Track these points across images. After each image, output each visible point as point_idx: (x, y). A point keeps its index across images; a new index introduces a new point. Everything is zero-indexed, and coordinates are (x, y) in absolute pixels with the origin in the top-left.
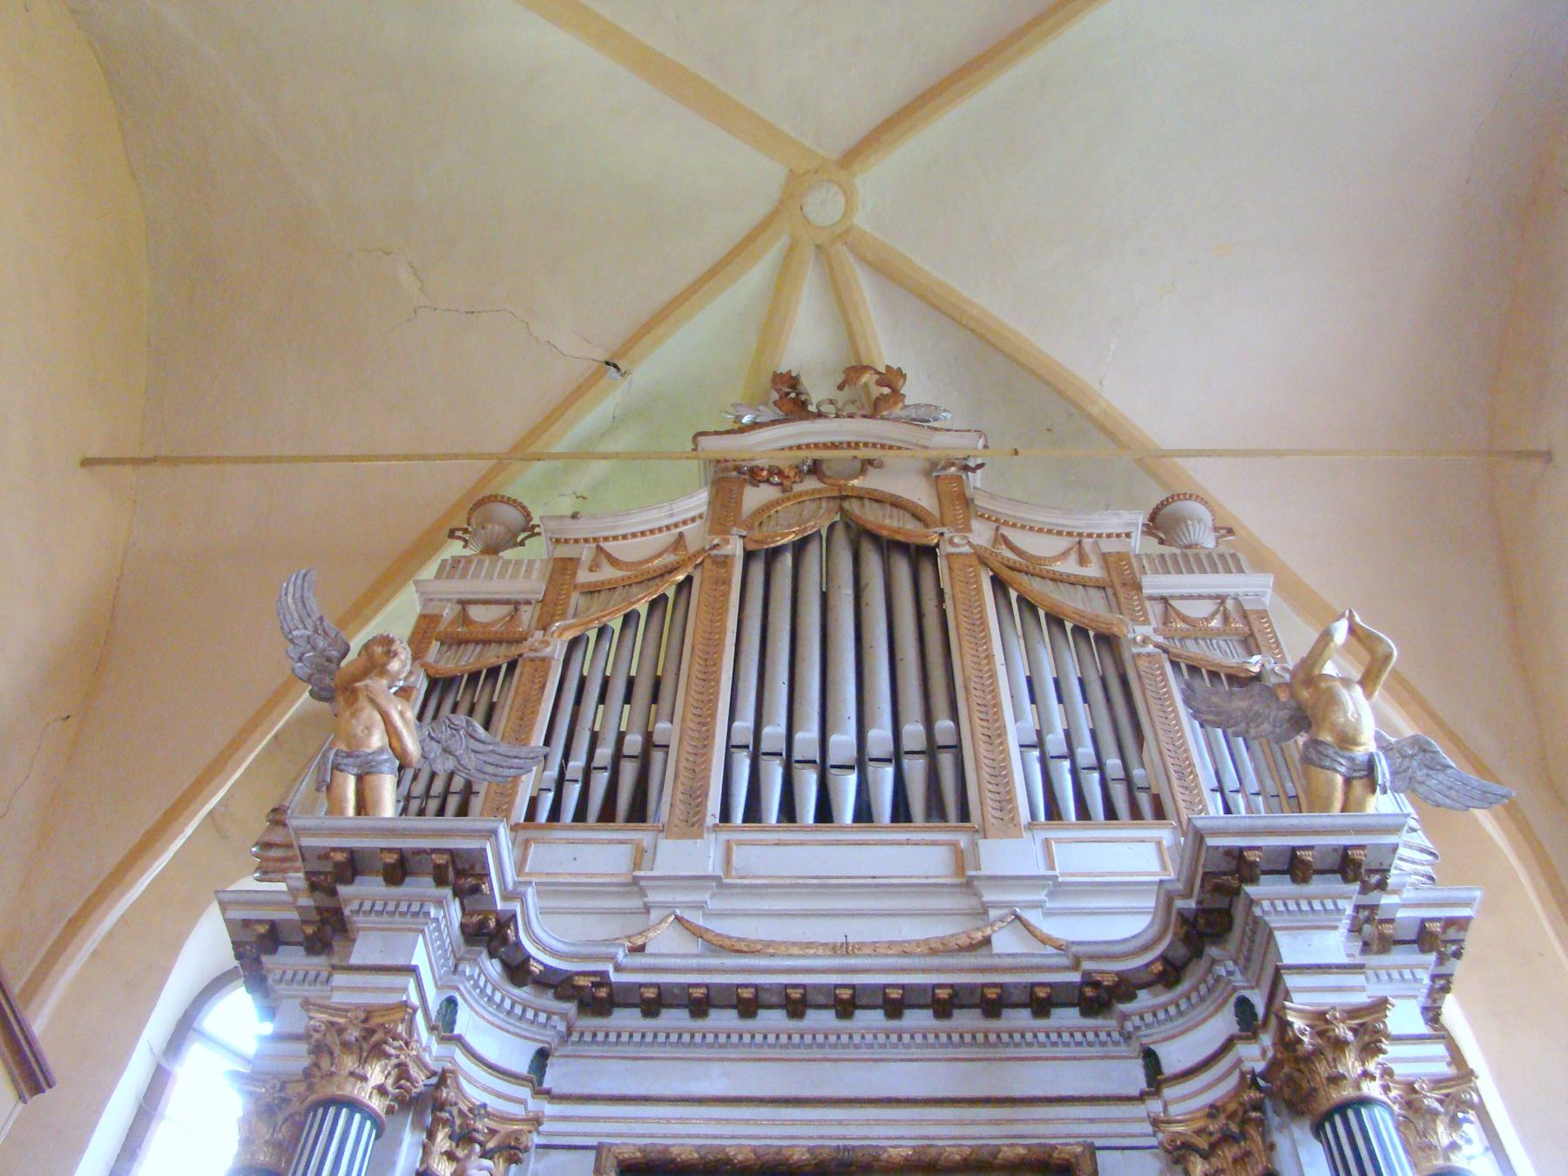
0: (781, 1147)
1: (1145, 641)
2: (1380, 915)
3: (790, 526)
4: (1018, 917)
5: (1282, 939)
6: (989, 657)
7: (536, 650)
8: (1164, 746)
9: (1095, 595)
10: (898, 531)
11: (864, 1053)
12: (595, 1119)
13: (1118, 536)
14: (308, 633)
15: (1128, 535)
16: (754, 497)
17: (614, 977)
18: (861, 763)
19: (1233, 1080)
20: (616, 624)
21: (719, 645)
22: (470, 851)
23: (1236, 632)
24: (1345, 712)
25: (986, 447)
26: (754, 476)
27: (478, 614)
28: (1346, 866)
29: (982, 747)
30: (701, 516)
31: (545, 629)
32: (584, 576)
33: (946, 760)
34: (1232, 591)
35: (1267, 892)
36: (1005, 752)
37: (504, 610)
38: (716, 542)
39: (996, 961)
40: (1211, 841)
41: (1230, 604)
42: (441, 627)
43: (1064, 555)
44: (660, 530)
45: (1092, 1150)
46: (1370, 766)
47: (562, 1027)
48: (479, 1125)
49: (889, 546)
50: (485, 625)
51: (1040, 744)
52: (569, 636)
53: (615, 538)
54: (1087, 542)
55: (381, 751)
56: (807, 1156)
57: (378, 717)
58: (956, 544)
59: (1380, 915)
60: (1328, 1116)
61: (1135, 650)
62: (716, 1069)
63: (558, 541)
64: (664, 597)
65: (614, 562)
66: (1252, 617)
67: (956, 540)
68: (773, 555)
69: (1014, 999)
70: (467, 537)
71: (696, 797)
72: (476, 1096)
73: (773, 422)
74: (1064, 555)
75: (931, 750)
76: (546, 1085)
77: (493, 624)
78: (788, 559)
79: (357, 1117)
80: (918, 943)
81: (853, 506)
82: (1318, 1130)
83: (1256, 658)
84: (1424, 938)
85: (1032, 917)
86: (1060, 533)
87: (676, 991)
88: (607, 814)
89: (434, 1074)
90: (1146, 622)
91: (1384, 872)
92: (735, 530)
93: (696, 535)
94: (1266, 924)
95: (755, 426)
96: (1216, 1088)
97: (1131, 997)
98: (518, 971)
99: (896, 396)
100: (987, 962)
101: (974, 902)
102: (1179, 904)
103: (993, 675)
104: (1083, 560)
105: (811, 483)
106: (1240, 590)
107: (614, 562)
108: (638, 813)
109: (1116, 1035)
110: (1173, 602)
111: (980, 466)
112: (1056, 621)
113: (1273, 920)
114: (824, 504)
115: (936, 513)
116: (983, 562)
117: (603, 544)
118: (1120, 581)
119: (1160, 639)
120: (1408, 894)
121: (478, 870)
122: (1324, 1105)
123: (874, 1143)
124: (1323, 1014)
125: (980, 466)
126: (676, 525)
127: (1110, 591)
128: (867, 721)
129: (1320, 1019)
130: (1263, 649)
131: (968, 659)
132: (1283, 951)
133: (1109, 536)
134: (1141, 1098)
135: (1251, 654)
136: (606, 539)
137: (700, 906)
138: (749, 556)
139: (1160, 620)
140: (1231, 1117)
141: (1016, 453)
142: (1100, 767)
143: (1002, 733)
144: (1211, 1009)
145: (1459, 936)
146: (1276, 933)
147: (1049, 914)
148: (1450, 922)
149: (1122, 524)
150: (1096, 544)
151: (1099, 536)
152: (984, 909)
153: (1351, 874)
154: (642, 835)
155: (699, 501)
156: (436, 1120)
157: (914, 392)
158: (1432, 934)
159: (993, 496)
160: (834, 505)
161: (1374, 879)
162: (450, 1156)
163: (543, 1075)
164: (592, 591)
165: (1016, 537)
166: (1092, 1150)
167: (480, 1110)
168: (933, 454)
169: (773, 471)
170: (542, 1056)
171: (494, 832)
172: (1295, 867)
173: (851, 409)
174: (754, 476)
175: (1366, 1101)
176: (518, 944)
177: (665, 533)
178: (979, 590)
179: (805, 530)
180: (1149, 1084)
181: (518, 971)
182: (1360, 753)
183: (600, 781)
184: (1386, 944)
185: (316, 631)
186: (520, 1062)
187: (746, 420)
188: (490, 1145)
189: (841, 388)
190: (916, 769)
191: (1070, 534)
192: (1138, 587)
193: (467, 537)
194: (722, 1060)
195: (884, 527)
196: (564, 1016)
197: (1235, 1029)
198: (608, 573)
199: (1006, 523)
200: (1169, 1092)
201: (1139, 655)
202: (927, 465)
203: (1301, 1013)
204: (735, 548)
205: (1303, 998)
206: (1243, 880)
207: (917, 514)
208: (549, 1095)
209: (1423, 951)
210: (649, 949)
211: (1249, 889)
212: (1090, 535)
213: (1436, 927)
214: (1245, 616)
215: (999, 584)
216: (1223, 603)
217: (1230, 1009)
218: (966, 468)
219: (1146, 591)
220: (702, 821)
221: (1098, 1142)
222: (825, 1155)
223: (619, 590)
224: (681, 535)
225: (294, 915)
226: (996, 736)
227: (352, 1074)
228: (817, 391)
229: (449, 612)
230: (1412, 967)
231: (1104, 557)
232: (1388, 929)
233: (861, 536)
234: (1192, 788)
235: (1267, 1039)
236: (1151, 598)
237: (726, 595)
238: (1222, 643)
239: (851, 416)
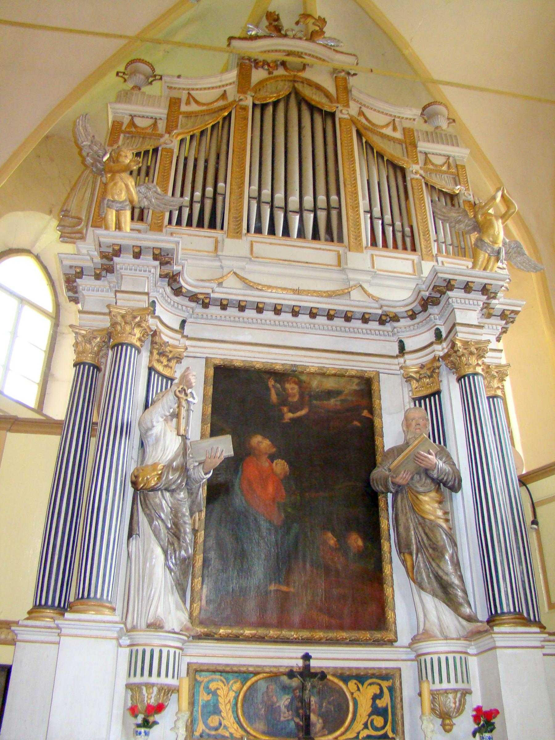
0: (272, 363)
1: (416, 173)
2: (491, 306)
3: (272, 93)
4: (361, 286)
5: (458, 313)
6: (354, 170)
7: (166, 144)
8: (419, 219)
9: (399, 146)
10: (319, 103)
11: (300, 330)
12: (205, 347)
13: (410, 119)
14: (89, 143)
15: (414, 120)
16: (258, 75)
17: (212, 295)
18: (301, 211)
19: (431, 357)
20: (198, 134)
21: (244, 149)
22: (168, 249)
23: (452, 174)
24: (494, 231)
25: (357, 64)
26: (257, 63)
28: (485, 290)
29: (350, 211)
30: (234, 83)
31: (169, 133)
33: (334, 213)
34: (453, 154)
36: (359, 214)
37: (151, 122)
38: (241, 98)
39: (352, 303)
40: (440, 275)
41: (451, 160)
42: (124, 128)
43: (387, 125)
44: (216, 87)
45: (378, 373)
46: (499, 252)
47: (191, 311)
48: (167, 350)
49: (313, 109)
50: (143, 129)
51: (371, 212)
52: (180, 138)
53: (197, 89)
54: (397, 119)
55: (125, 201)
56: (281, 367)
57: (124, 185)
58: (342, 114)
59: (491, 306)
60: (464, 377)
61: (413, 176)
62: (247, 332)
63: (171, 88)
64: (219, 122)
65: (197, 102)
66: (459, 167)
67: (343, 111)
68: (264, 107)
69: (356, 317)
70: (126, 77)
72: (166, 339)
73: (265, 37)
74: (387, 125)
75: (328, 209)
76: (185, 334)
77: (147, 128)
78: (270, 109)
79: (134, 349)
80: (325, 292)
81: (299, 86)
82: (459, 380)
83: (458, 187)
84: (503, 315)
85: (365, 286)
86: (387, 114)
87: (234, 302)
89: (152, 331)
90: (417, 163)
91: (496, 293)
92: (249, 92)
93: (232, 94)
94: (452, 306)
95: (256, 37)
96: (425, 358)
97: (398, 321)
99: (322, 32)
100: (348, 302)
101: (344, 277)
102: (423, 293)
103: (355, 179)
104: (395, 129)
105: (281, 71)
106: (456, 154)
107: (197, 102)
109: (391, 334)
110: (429, 155)
111: (355, 74)
112: (380, 156)
113: (455, 305)
114: (287, 83)
115: (335, 95)
116: (354, 123)
117: (191, 92)
118: (409, 142)
120: (502, 300)
121: (170, 256)
122: (463, 373)
123: (304, 364)
124: (468, 342)
125: (355, 74)
126: (223, 86)
127: (404, 146)
128: (303, 192)
129: (466, 344)
130: (462, 183)
131: (346, 170)
132: (457, 317)
133: (407, 119)
134: (397, 357)
135: (456, 185)
136: (193, 89)
137: (243, 269)
138: (254, 105)
139: (423, 163)
140: (429, 369)
141: (372, 71)
142: (393, 225)
143: (358, 207)
144: (426, 330)
145: (514, 316)
146: (456, 310)
147: (371, 285)
148: (513, 311)
149: (411, 113)
150: (401, 122)
151: (403, 118)
152: (348, 280)
153: (485, 293)
154: (217, 233)
155: (232, 75)
156: (153, 348)
157: (328, 31)
158: (507, 315)
159: (361, 92)
160: (291, 84)
161: (492, 295)
162: (159, 361)
163: (184, 329)
164: (188, 115)
165: (369, 113)
166: (378, 373)
167: (167, 344)
168: (336, 65)
169: (265, 63)
170: (184, 322)
171: (179, 243)
172: (467, 288)
173: (299, 35)
174: (257, 63)
175: (477, 374)
176: (179, 282)
177: (218, 90)
178: (351, 137)
179: (279, 96)
180: (399, 352)
181: (178, 292)
182: (496, 247)
183: (197, 207)
184: (489, 316)
185: (92, 142)
186: (177, 326)
187: (253, 33)
188: (170, 356)
189: (297, 23)
190: (322, 215)
191: (391, 115)
192: (415, 146)
193: (126, 77)
194: (249, 328)
195: (314, 101)
196: (192, 308)
197: (433, 339)
198: (194, 107)
199: (365, 106)
200: (406, 356)
201: (413, 179)
202: (332, 70)
203: (461, 341)
204: (249, 102)
205: (462, 335)
206: (448, 290)
207: (327, 95)
208: (187, 337)
209: (501, 319)
210: (224, 285)
211: (449, 293)
212: (399, 117)
213: (507, 313)
214: (457, 166)
215: (359, 135)
216: (448, 159)
217: (432, 332)
218: (349, 74)
219: (419, 149)
220: (241, 233)
221: (381, 371)
222: (287, 367)
223: (199, 117)
224: (225, 91)
225: (91, 265)
226: (356, 207)
227: (130, 333)
228: (287, 23)
229: (126, 121)
230: (496, 325)
231: (404, 129)
232: (491, 311)
233: (302, 101)
234: (428, 240)
235: (444, 344)
236: (421, 152)
237: (246, 125)
238: (446, 178)
239: (300, 39)
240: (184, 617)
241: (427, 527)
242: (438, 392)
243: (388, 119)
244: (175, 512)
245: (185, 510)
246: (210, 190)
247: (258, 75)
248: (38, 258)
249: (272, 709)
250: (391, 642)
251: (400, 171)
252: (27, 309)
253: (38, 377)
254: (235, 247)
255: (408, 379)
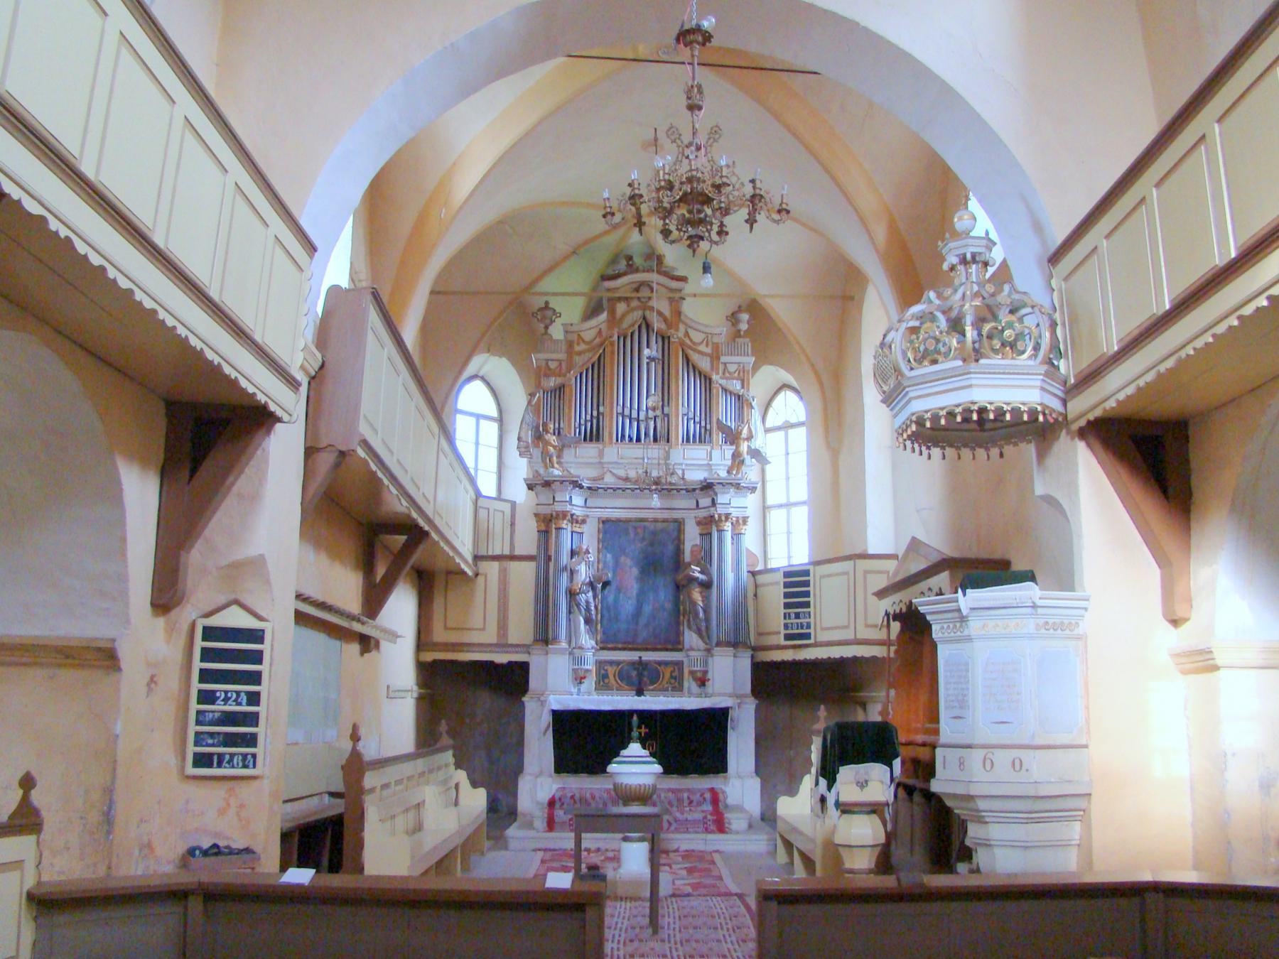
18: (647, 418)
26: (619, 299)
27: (553, 365)
32: (577, 348)
35: (717, 488)
71: (611, 438)
88: (591, 440)
98: (581, 487)
108: (598, 439)
118: (715, 357)
119: (723, 382)
129: (720, 515)
164: (580, 353)
165: (692, 333)
174: (619, 299)
181: (581, 487)
192: (718, 358)
198: (583, 347)
240: (593, 643)
241: (694, 603)
242: (710, 534)
243: (703, 336)
244: (587, 602)
245: (591, 600)
246: (595, 413)
247: (621, 308)
248: (483, 379)
249: (629, 677)
250: (681, 650)
251: (707, 380)
252: (482, 422)
253: (495, 469)
254: (612, 452)
255: (699, 523)
